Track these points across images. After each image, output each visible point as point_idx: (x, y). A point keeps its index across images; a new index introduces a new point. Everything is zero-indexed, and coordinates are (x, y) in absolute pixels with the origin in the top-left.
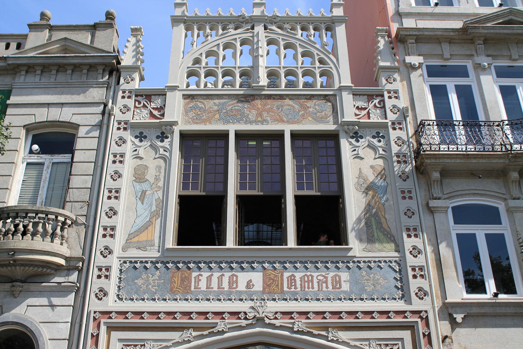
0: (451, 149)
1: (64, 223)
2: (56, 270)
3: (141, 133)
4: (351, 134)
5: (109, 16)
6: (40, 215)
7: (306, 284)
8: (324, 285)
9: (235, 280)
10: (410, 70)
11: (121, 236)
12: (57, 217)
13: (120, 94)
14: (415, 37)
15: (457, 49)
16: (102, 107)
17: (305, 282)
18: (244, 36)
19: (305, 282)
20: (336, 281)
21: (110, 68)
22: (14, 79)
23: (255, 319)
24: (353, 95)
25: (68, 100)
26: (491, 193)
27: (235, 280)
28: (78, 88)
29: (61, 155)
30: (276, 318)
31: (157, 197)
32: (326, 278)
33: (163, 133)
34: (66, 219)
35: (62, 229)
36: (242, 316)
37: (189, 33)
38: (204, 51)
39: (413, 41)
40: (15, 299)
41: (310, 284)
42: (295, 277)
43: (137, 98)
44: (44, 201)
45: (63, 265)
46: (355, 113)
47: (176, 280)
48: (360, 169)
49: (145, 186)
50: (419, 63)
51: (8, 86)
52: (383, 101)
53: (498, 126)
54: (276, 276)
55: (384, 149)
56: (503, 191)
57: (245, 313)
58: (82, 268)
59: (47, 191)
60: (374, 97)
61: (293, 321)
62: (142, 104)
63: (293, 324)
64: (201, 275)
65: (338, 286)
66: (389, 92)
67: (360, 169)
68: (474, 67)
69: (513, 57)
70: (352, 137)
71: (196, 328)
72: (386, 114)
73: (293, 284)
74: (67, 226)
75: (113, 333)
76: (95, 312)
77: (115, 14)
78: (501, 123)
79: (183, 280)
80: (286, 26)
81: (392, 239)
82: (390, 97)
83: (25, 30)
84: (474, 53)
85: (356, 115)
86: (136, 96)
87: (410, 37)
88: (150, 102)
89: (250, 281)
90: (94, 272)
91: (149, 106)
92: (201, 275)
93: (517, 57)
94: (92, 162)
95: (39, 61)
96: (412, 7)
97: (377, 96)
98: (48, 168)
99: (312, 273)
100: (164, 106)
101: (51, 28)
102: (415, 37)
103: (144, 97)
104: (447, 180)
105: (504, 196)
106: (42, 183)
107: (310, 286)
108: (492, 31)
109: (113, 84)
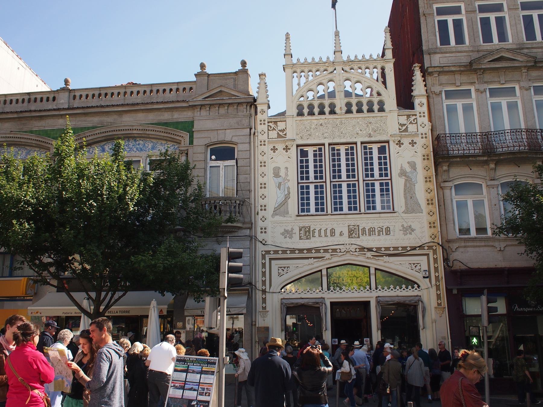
0: (454, 153)
1: (239, 204)
2: (238, 229)
3: (274, 147)
4: (396, 142)
5: (244, 63)
6: (227, 201)
7: (372, 232)
8: (381, 233)
9: (333, 231)
10: (434, 95)
11: (270, 209)
12: (235, 201)
13: (259, 122)
14: (438, 73)
15: (464, 78)
16: (249, 129)
17: (371, 231)
18: (330, 76)
19: (371, 231)
20: (388, 231)
21: (250, 104)
22: (194, 113)
23: (345, 252)
24: (398, 115)
25: (229, 127)
26: (478, 176)
27: (333, 231)
28: (233, 119)
29: (229, 161)
30: (356, 251)
31: (287, 186)
32: (382, 229)
33: (287, 146)
34: (240, 202)
35: (239, 207)
36: (338, 251)
37: (295, 75)
38: (305, 89)
39: (437, 75)
40: (219, 245)
41: (374, 232)
42: (365, 229)
43: (269, 124)
44: (224, 189)
45: (242, 227)
46: (399, 128)
47: (302, 232)
48: (402, 164)
49: (280, 180)
50: (440, 91)
51: (191, 118)
52: (416, 118)
53: (485, 135)
54: (355, 229)
55: (416, 151)
56: (485, 174)
57: (340, 249)
58: (252, 228)
59: (224, 183)
60: (411, 116)
61: (365, 253)
62: (272, 128)
63: (365, 254)
64: (316, 230)
65: (389, 233)
66: (420, 113)
67: (402, 164)
68: (475, 90)
69: (501, 83)
70: (397, 144)
71: (315, 258)
72: (417, 128)
73: (365, 233)
74: (241, 206)
75: (272, 261)
76: (262, 251)
77: (247, 62)
78: (487, 134)
79: (306, 232)
80: (356, 67)
81: (419, 206)
82: (420, 116)
83: (194, 79)
84: (476, 81)
85: (399, 129)
86: (268, 122)
87: (434, 73)
88: (277, 126)
89: (342, 232)
90: (259, 230)
91: (276, 129)
92: (316, 230)
93: (504, 82)
94: (248, 166)
95: (208, 103)
96: (437, 48)
97: (413, 115)
98: (222, 169)
99: (375, 227)
100: (286, 128)
101: (209, 75)
102: (438, 73)
103: (273, 123)
104: (452, 169)
105: (486, 178)
106: (221, 178)
107: (374, 234)
108: (488, 66)
109: (253, 115)
